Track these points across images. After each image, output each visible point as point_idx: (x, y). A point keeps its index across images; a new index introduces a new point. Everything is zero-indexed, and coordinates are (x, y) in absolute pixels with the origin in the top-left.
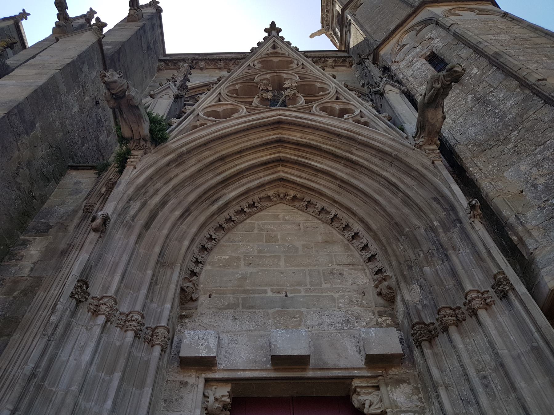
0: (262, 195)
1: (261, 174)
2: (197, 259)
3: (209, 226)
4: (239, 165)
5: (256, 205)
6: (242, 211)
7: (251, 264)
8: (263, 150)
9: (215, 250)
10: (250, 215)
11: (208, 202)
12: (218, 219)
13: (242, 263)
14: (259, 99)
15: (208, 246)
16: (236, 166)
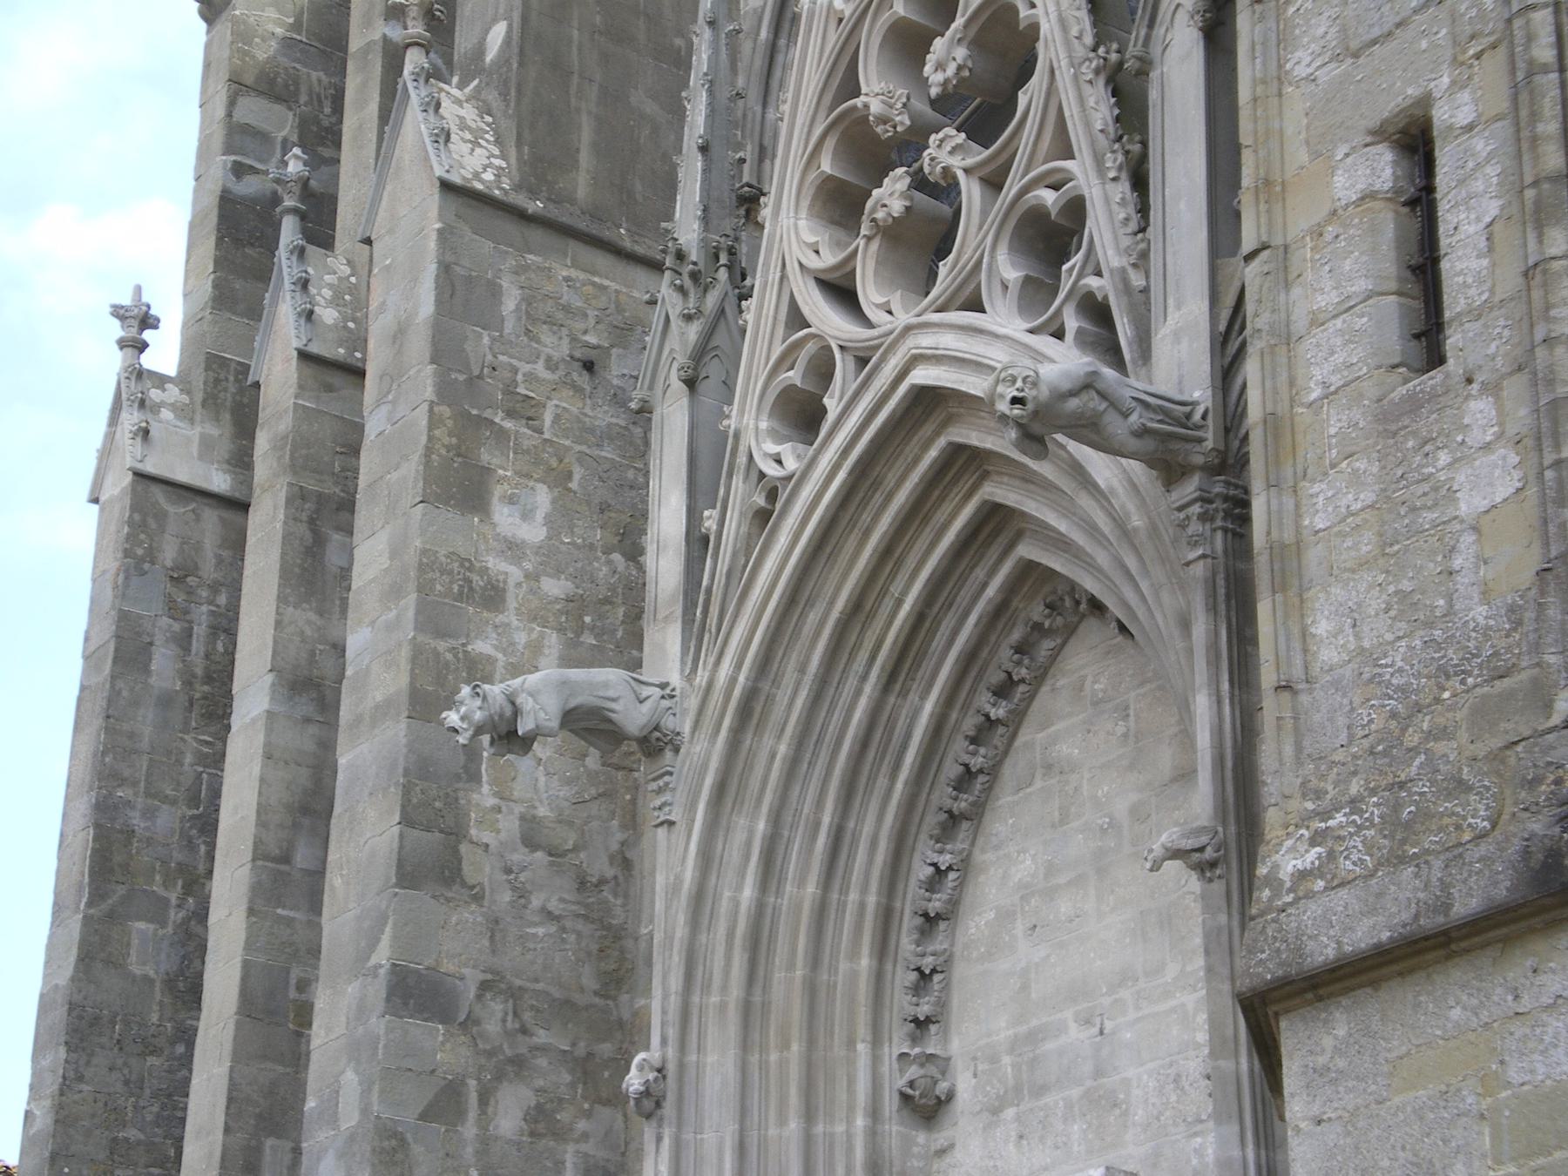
0: (1016, 636)
1: (980, 573)
2: (918, 969)
3: (923, 837)
4: (905, 592)
5: (1015, 678)
6: (990, 723)
7: (1035, 926)
8: (942, 499)
9: (967, 900)
10: (1017, 719)
11: (885, 768)
12: (935, 797)
13: (1020, 927)
14: (875, 245)
15: (936, 905)
16: (899, 602)
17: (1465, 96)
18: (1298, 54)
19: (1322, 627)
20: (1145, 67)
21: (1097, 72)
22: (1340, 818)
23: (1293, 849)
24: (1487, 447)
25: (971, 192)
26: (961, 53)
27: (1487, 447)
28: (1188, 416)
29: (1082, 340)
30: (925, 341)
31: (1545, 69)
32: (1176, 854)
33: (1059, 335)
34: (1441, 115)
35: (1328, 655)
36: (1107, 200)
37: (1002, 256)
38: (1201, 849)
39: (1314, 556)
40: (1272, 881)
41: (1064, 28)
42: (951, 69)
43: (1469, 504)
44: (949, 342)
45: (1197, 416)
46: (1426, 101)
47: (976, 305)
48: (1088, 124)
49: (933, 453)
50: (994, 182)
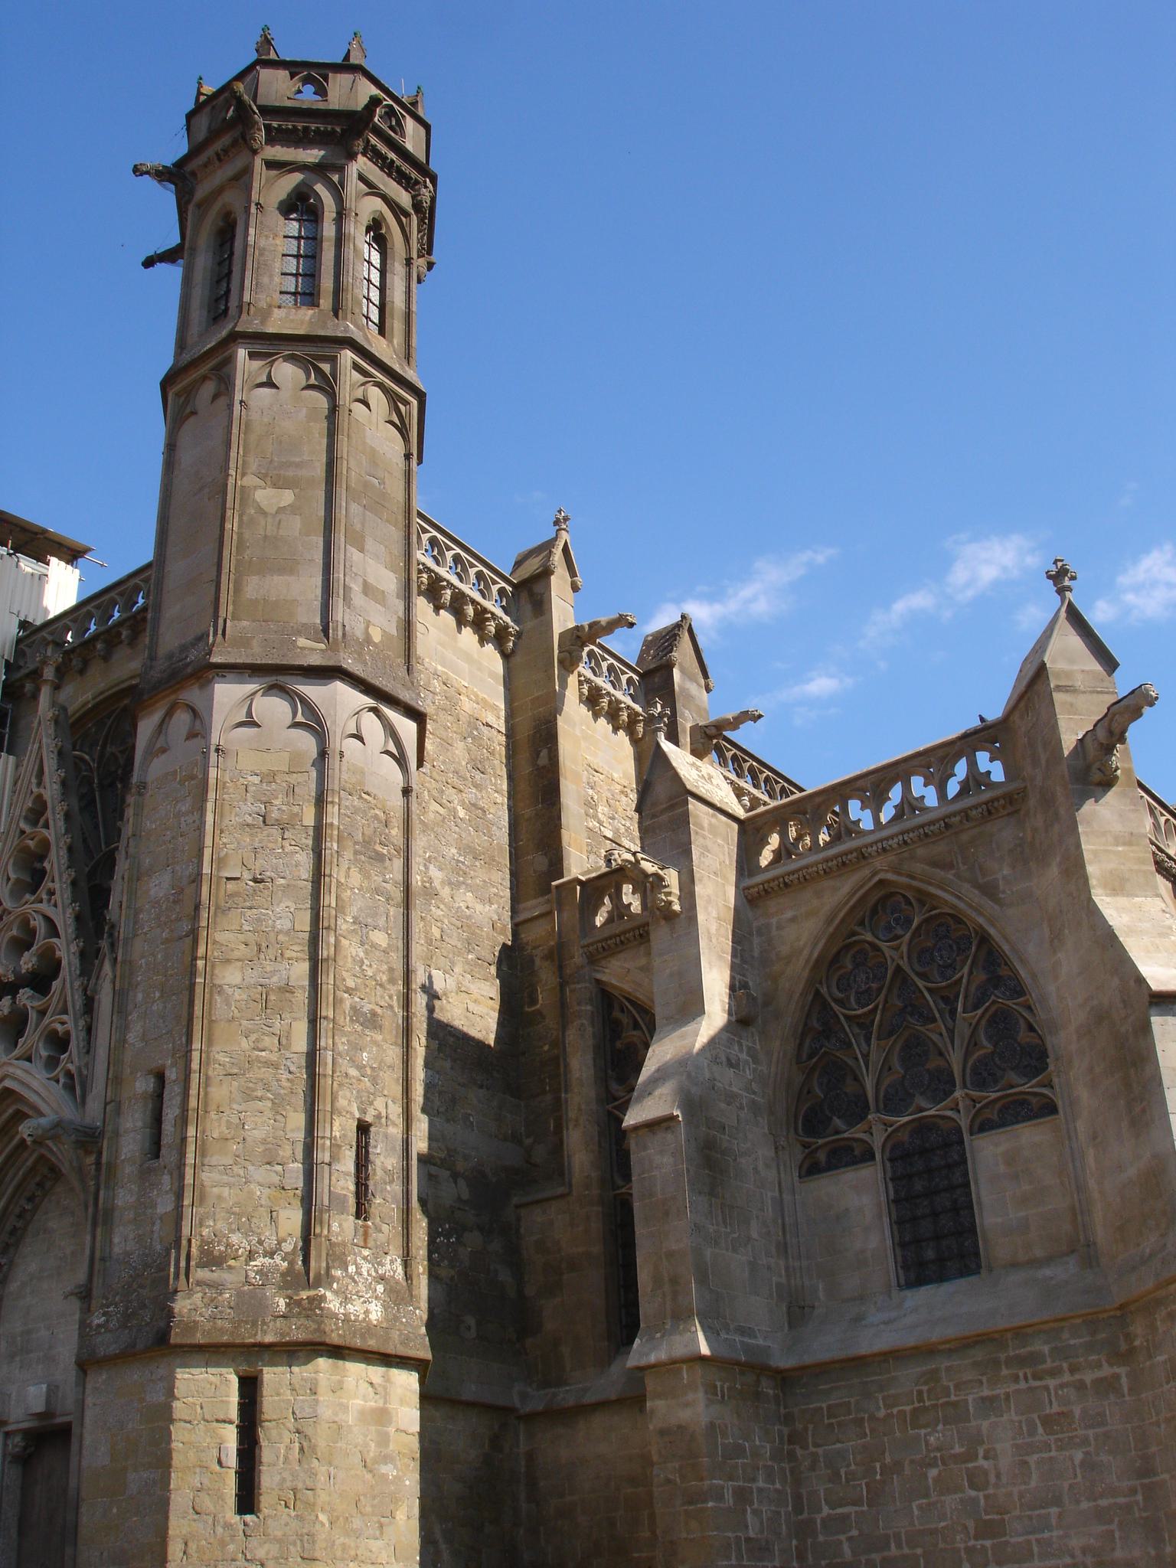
17: (174, 1069)
18: (131, 1035)
19: (116, 1240)
20: (95, 991)
21: (79, 986)
22: (111, 1309)
23: (97, 1316)
24: (167, 1192)
25: (33, 1016)
26: (34, 959)
27: (167, 1192)
28: (94, 1133)
29: (65, 1086)
30: (11, 1070)
31: (195, 1072)
32: (72, 1294)
33: (58, 1081)
34: (167, 1073)
35: (117, 1250)
36: (77, 1038)
37: (41, 1045)
38: (81, 1292)
39: (117, 1214)
40: (90, 1325)
41: (70, 967)
42: (30, 965)
43: (160, 1210)
44: (19, 1072)
45: (97, 1134)
46: (164, 1066)
47: (29, 1059)
48: (74, 1007)
49: (10, 1111)
50: (42, 1013)
